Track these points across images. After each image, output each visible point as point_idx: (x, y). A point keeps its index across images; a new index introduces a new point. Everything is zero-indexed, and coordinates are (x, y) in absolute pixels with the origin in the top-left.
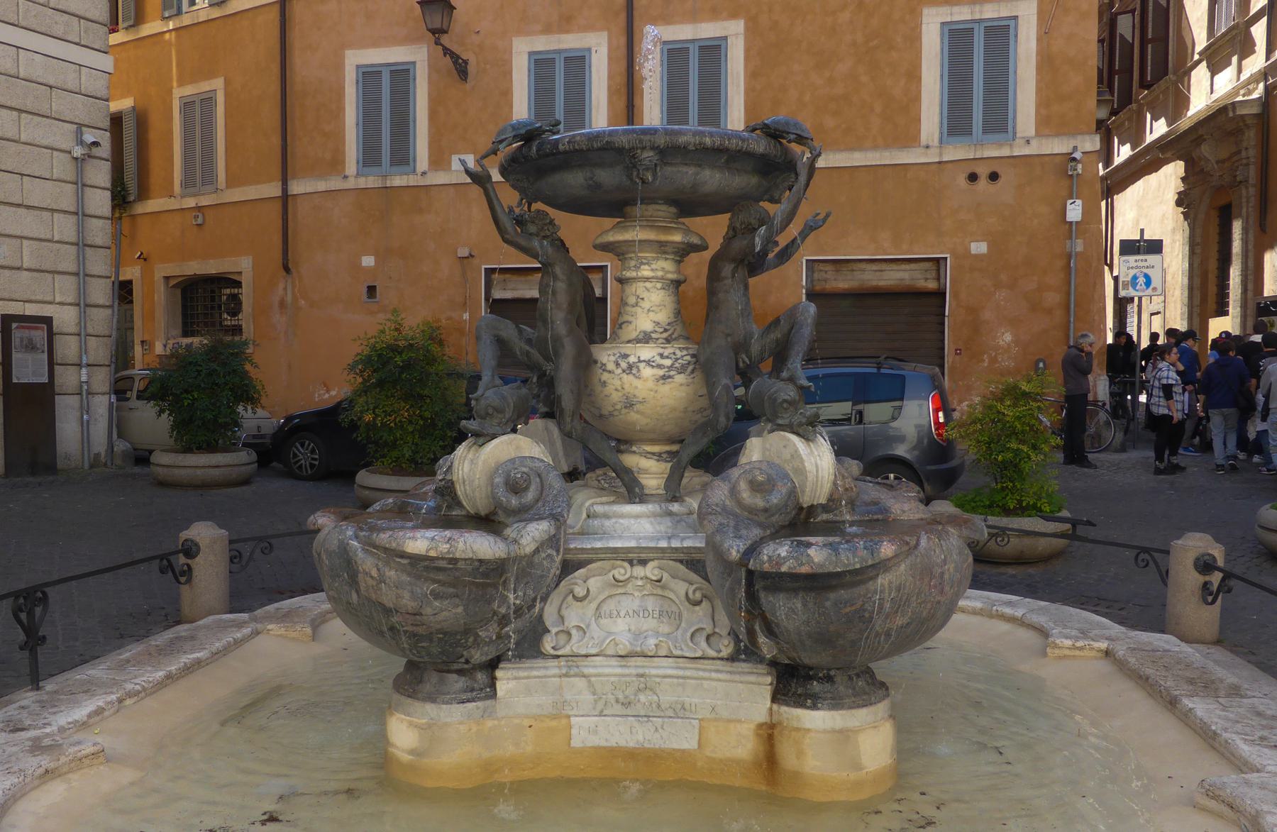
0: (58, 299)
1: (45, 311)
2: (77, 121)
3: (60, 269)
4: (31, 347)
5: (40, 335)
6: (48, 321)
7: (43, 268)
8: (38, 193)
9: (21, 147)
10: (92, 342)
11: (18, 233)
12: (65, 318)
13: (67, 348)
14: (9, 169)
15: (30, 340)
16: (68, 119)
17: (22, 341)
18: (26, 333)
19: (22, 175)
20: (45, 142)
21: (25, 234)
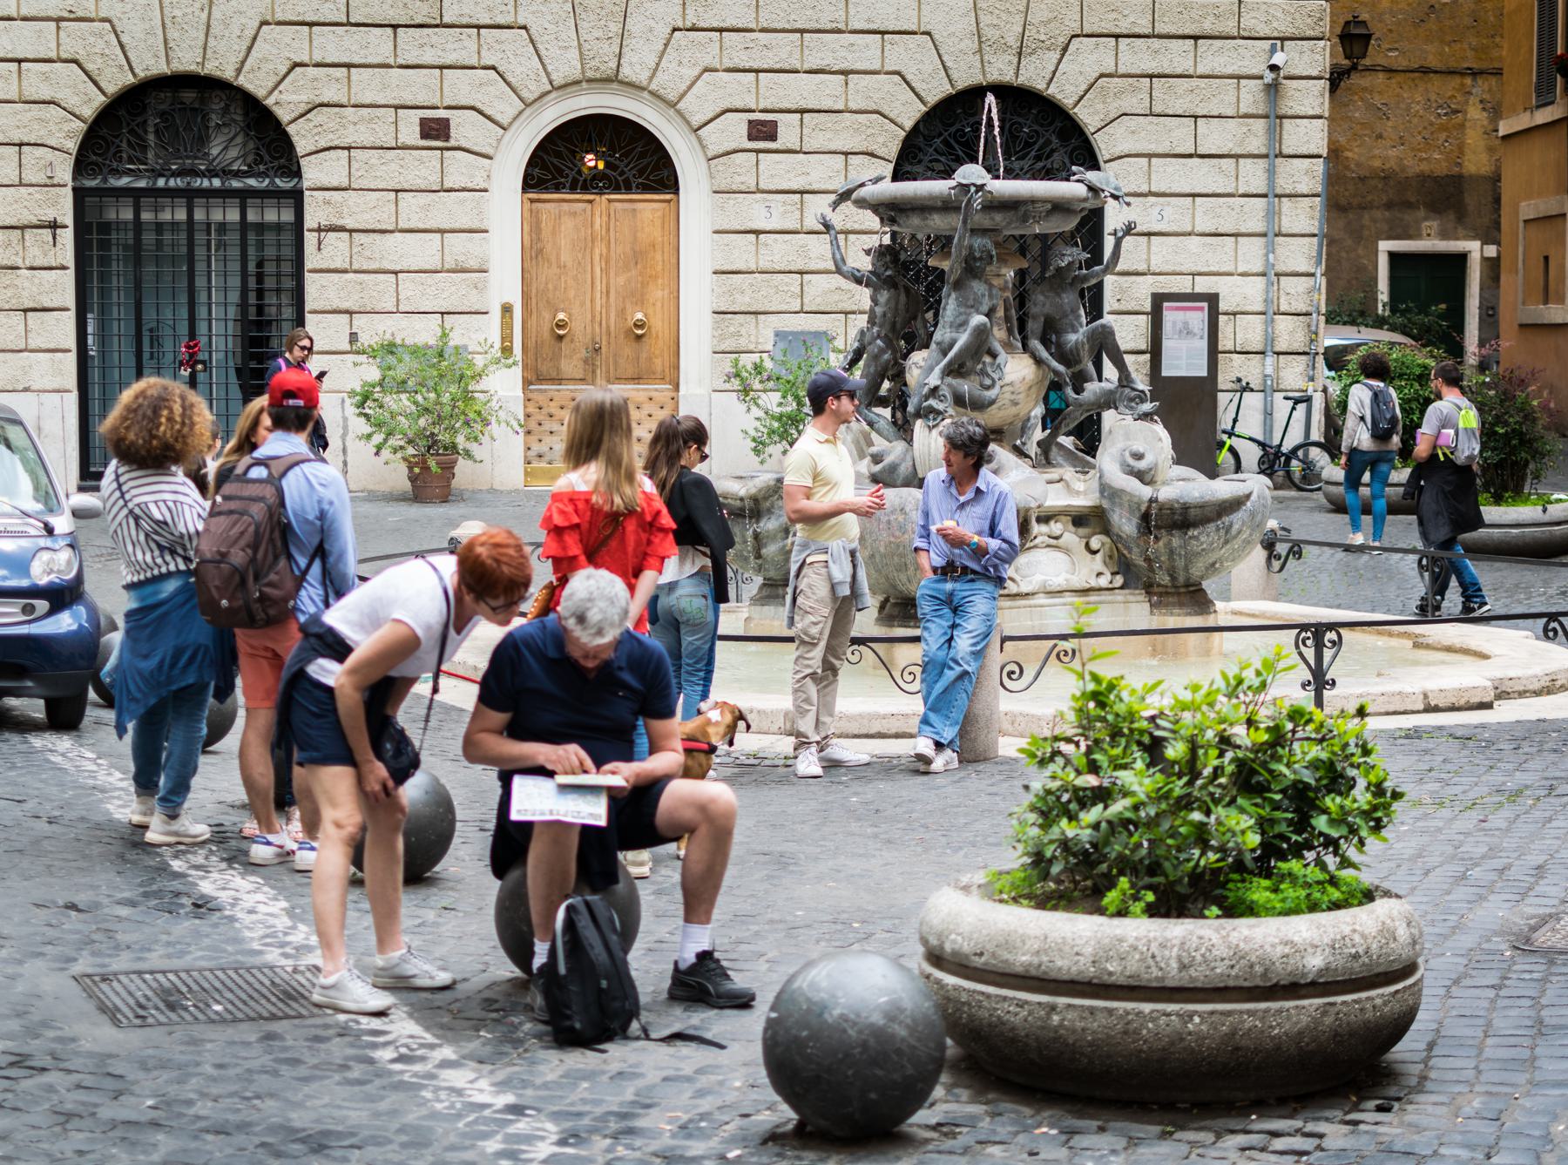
0: (1240, 270)
1: (1203, 285)
2: (1276, 34)
3: (1243, 230)
4: (1187, 332)
5: (1198, 319)
6: (1212, 299)
7: (1221, 230)
8: (1215, 137)
9: (1195, 82)
10: (1283, 324)
11: (1188, 190)
12: (1237, 293)
13: (1241, 332)
14: (1180, 112)
15: (1186, 324)
16: (1262, 34)
17: (1174, 323)
18: (1180, 316)
19: (1196, 117)
20: (1229, 71)
21: (1197, 190)
